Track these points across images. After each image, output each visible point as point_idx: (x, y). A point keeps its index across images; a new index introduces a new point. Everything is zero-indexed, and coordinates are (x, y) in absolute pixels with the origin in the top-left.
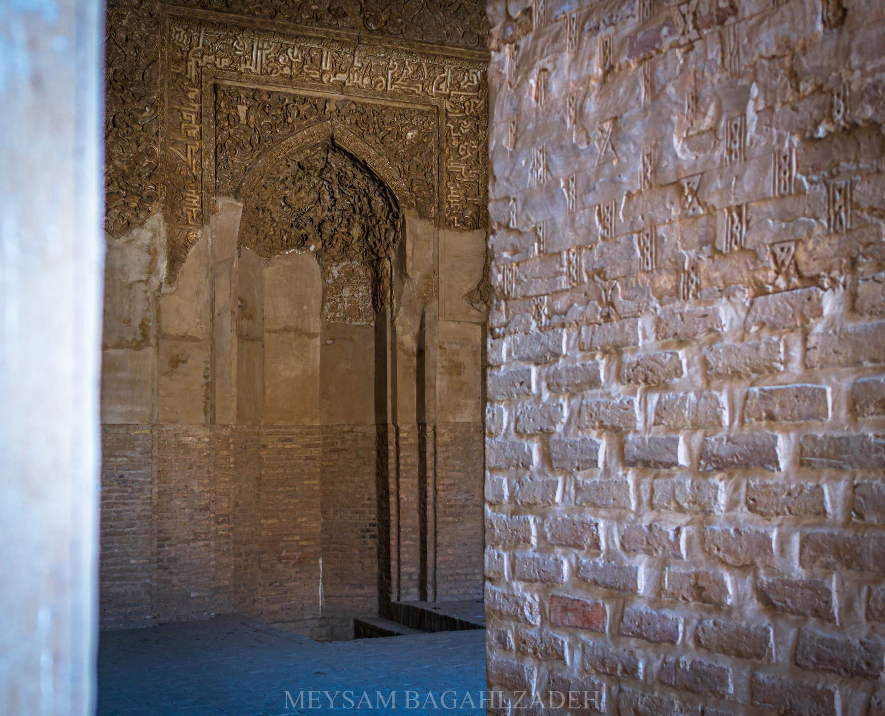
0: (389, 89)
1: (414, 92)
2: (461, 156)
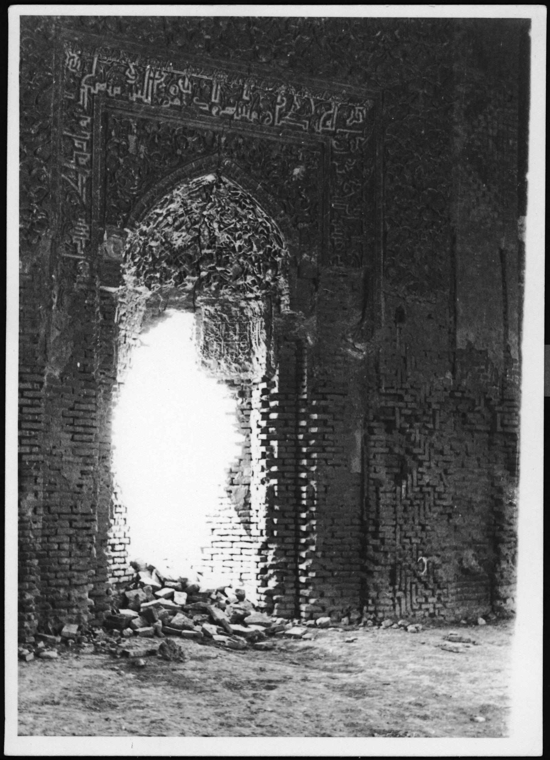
0: (276, 124)
1: (300, 128)
2: (345, 194)
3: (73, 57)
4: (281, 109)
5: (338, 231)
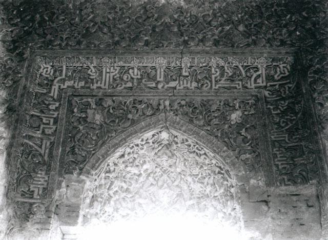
0: (214, 87)
1: (236, 88)
2: (283, 127)
3: (47, 68)
4: (216, 78)
5: (280, 157)
